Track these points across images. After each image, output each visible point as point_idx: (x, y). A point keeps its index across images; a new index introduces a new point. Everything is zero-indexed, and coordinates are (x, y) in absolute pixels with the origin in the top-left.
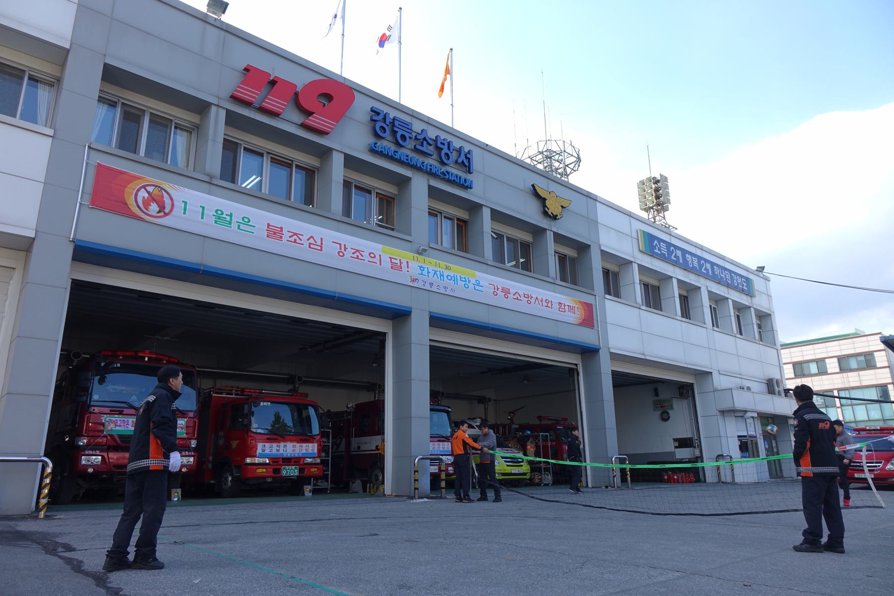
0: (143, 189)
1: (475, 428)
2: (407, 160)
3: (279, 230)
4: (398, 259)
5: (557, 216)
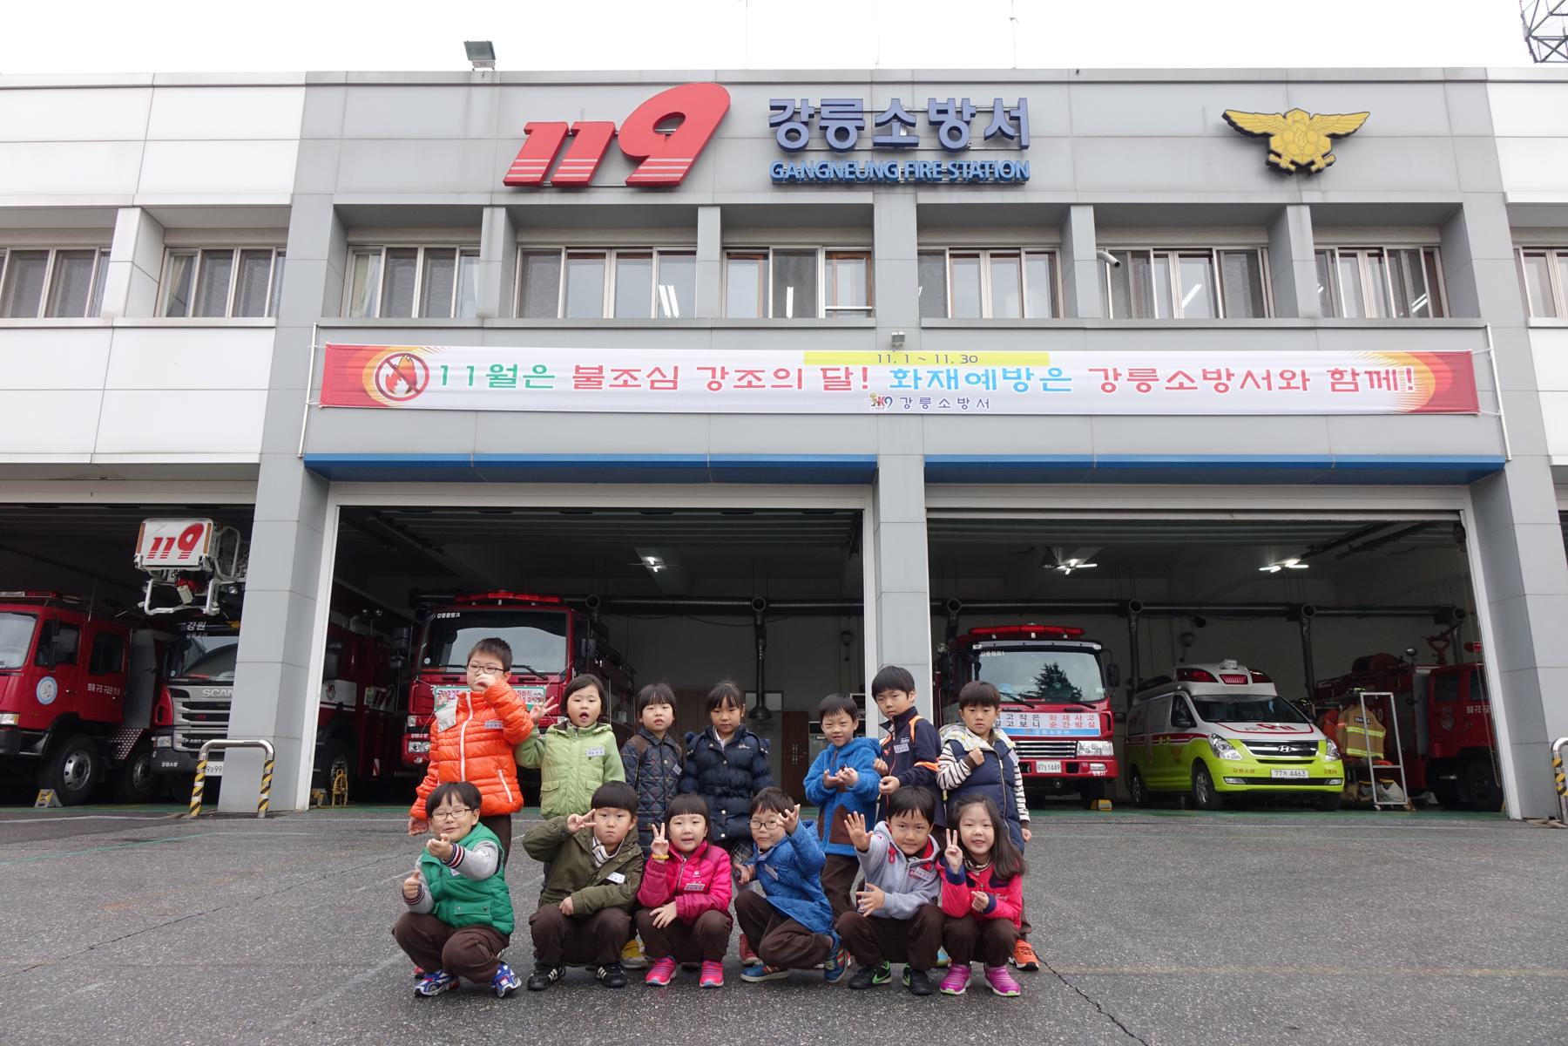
0: (386, 364)
2: (851, 173)
3: (597, 371)
4: (843, 368)
5: (1312, 163)
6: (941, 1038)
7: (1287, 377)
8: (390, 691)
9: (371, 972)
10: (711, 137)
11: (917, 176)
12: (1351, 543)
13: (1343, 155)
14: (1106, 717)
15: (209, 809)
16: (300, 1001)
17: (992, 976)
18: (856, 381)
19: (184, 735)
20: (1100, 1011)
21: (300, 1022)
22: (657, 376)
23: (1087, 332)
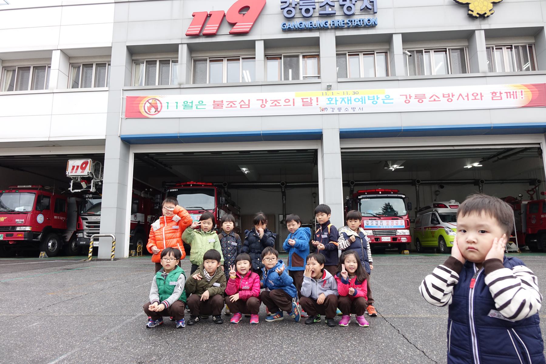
0: (147, 103)
1: (447, 208)
2: (311, 25)
3: (221, 102)
5: (485, 13)
6: (337, 344)
7: (475, 95)
8: (156, 217)
9: (133, 318)
10: (259, 15)
11: (335, 25)
12: (498, 157)
13: (498, 10)
14: (407, 221)
15: (95, 258)
16: (106, 329)
17: (358, 319)
18: (314, 102)
19: (87, 233)
20: (399, 333)
21: (103, 338)
22: (242, 103)
23: (400, 81)
